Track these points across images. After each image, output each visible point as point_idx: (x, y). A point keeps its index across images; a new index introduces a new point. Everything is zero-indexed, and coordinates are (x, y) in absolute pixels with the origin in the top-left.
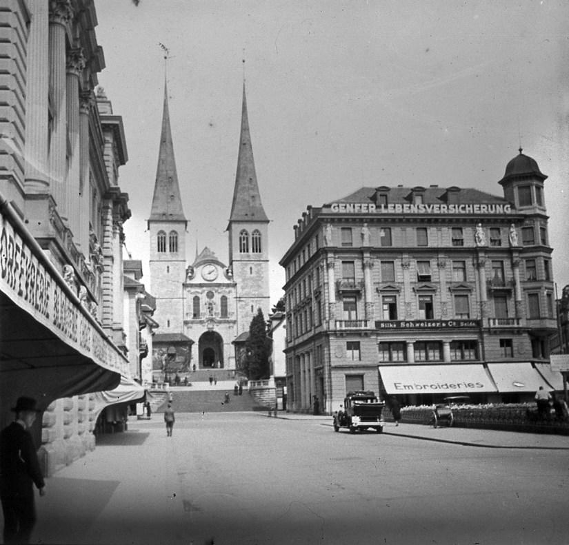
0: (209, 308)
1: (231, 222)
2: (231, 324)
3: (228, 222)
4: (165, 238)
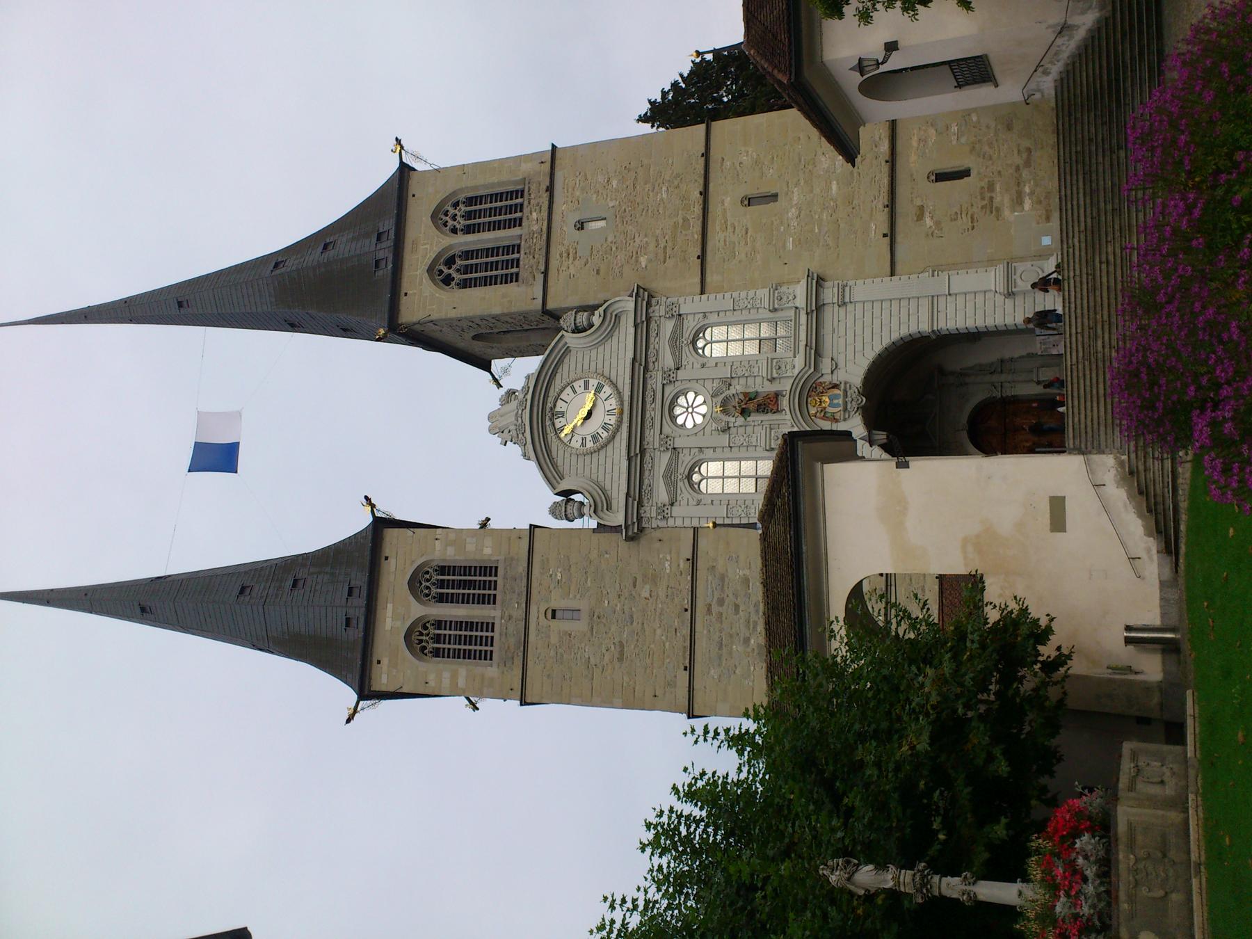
0: (744, 412)
2: (829, 294)
4: (439, 624)
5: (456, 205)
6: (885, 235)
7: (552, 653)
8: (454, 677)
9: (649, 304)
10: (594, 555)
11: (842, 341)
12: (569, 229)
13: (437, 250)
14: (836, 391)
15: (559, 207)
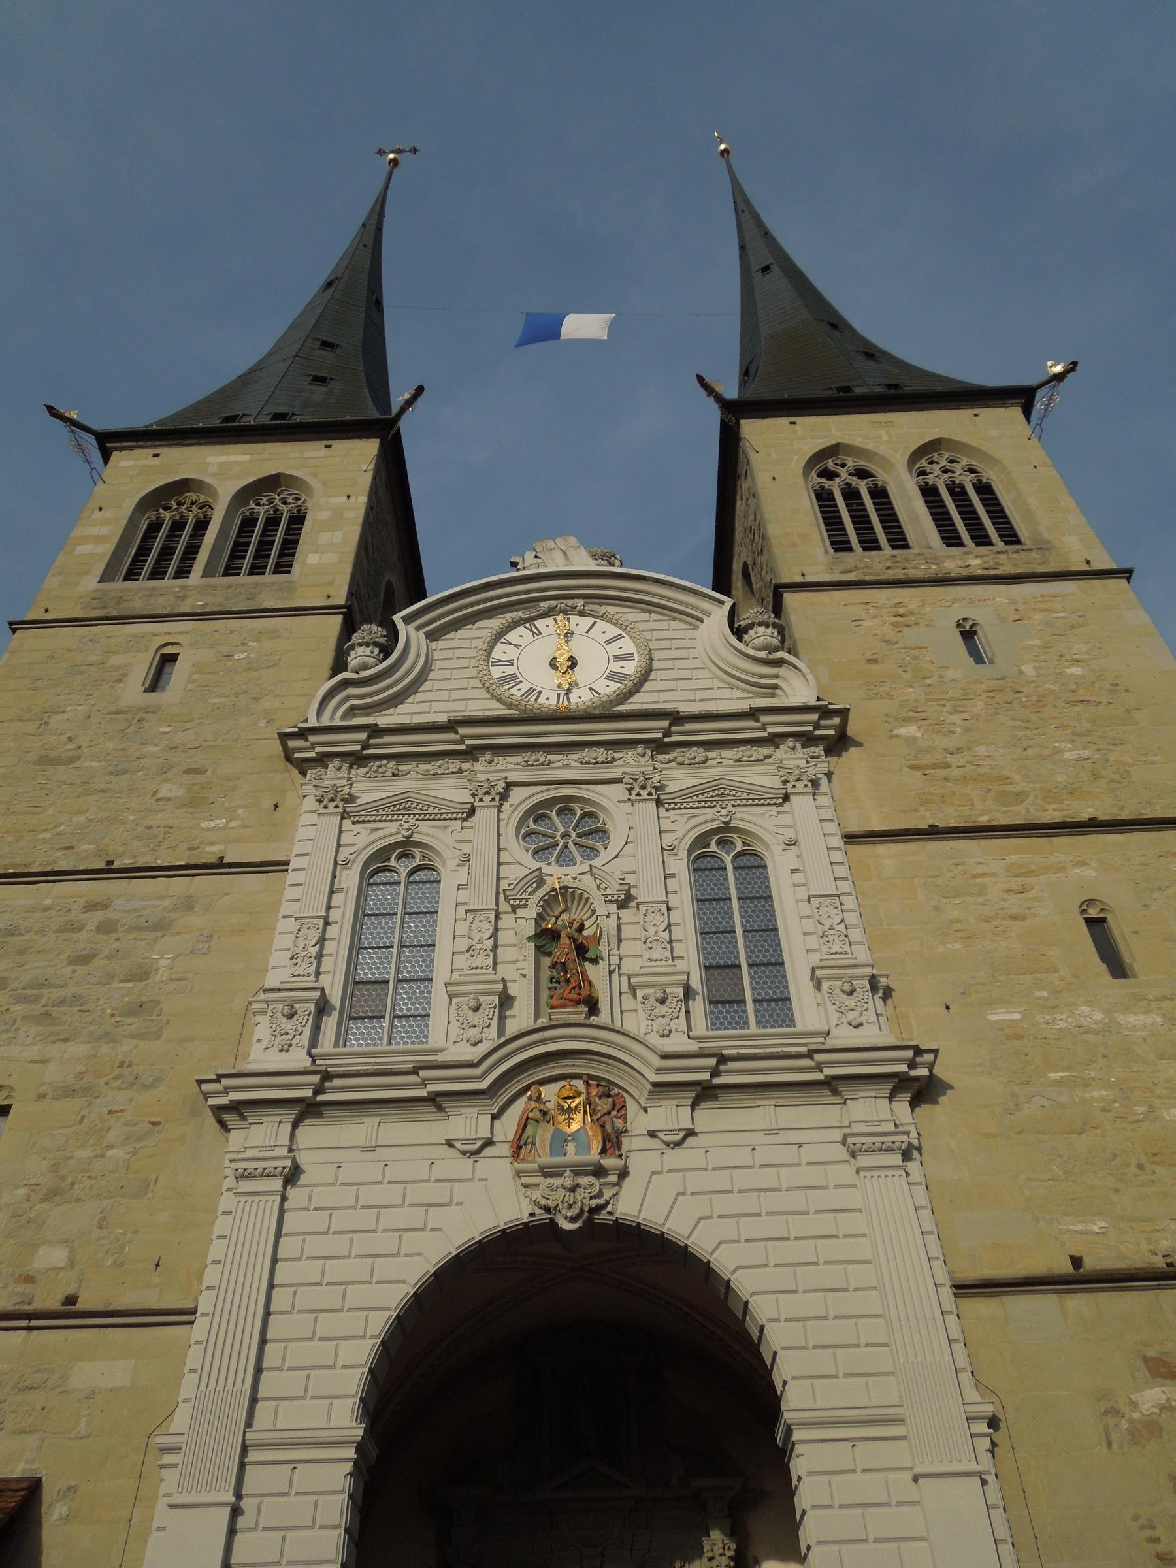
1: (734, 413)
2: (870, 1110)
3: (713, 415)
5: (972, 471)
6: (1076, 1261)
7: (92, 658)
8: (98, 539)
9: (807, 740)
10: (267, 703)
11: (744, 1157)
12: (958, 612)
13: (882, 450)
14: (596, 1145)
15: (1001, 594)
